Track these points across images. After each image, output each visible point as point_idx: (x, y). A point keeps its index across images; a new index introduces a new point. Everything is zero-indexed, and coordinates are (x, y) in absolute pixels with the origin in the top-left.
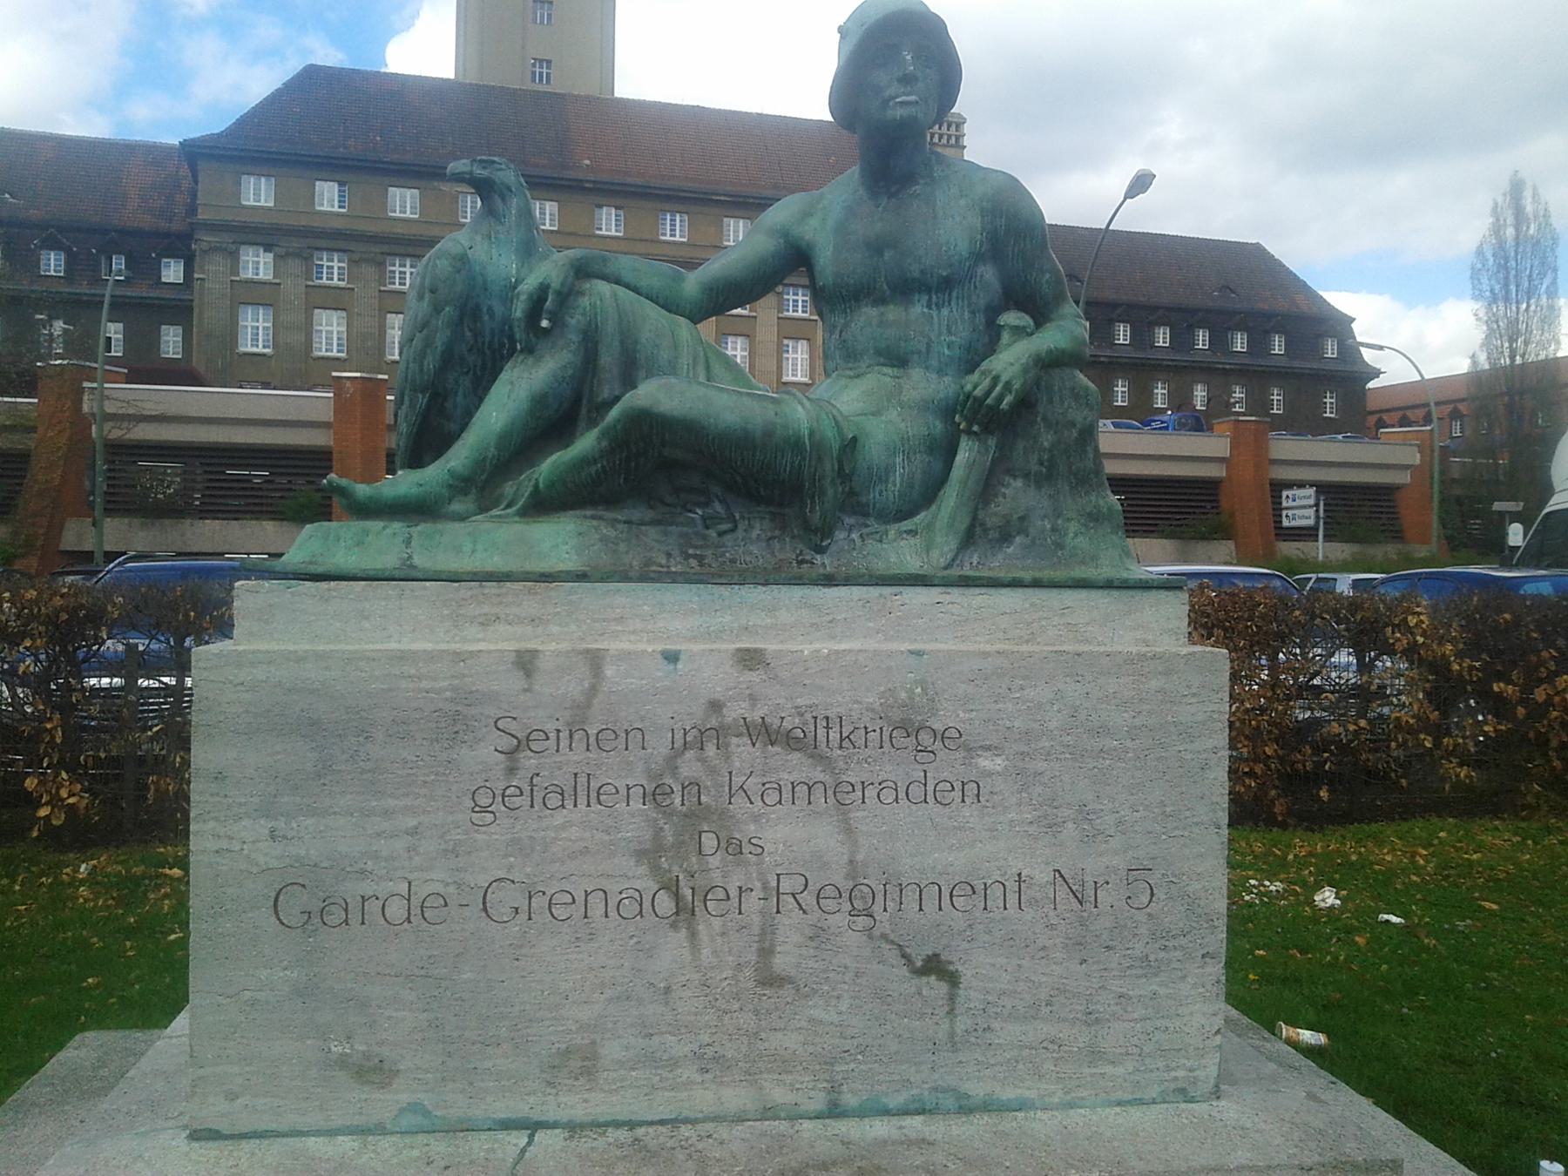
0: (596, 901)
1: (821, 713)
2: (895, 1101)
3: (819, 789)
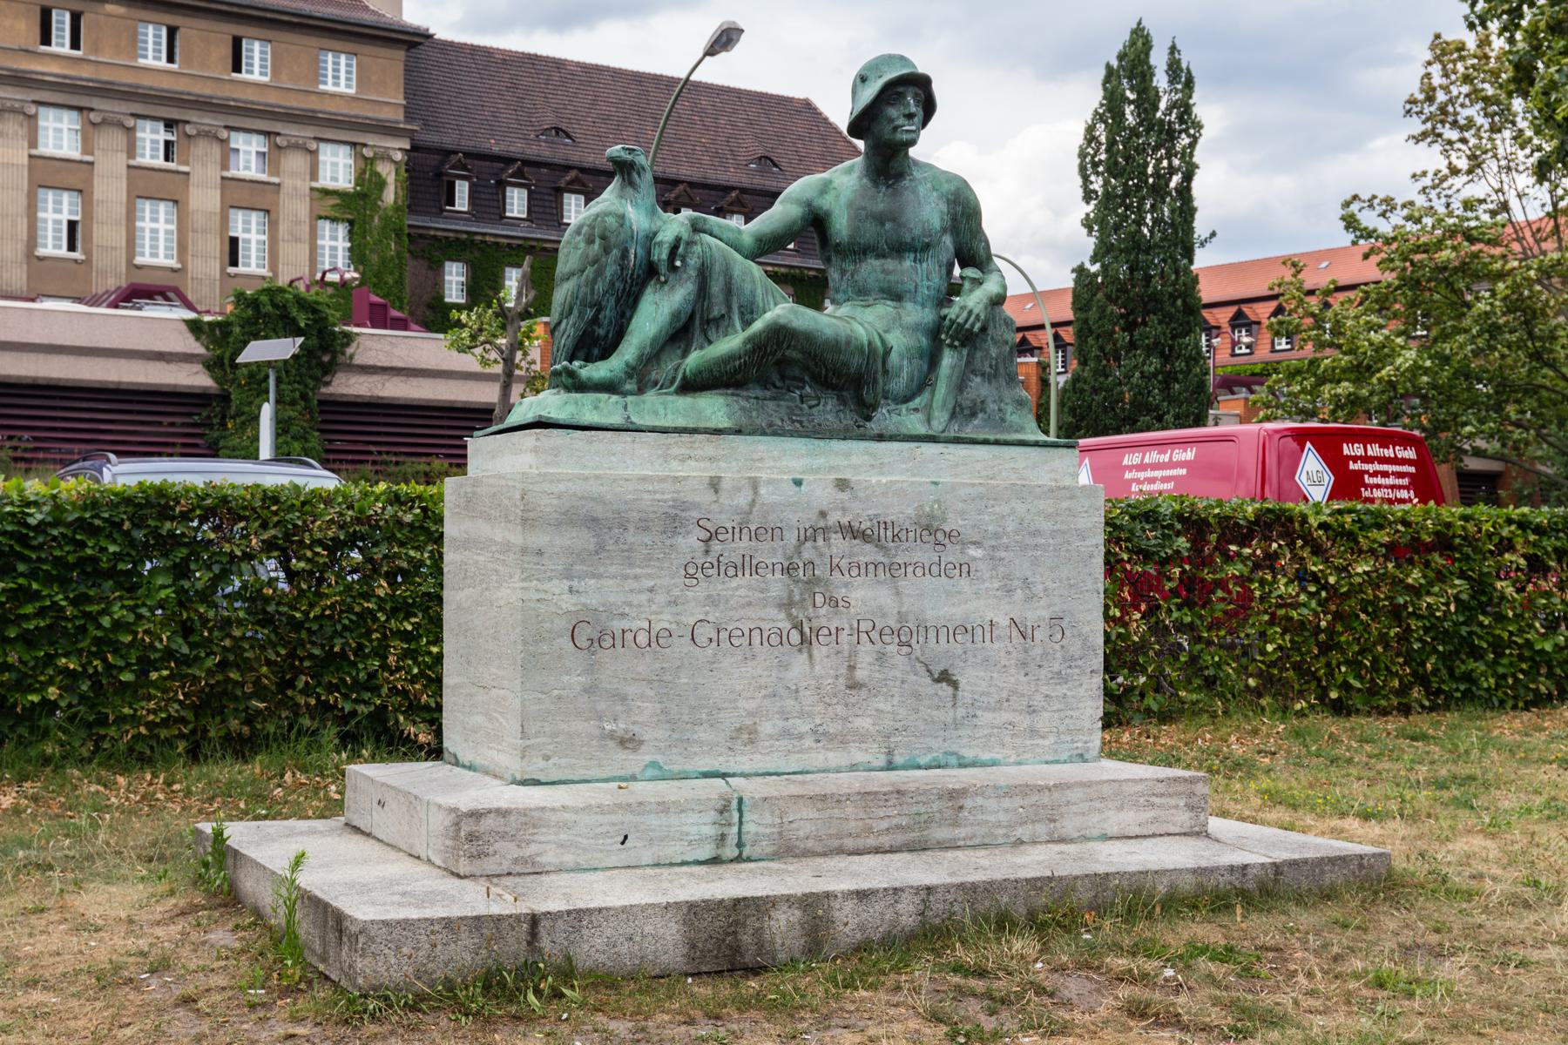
0: (756, 633)
1: (882, 519)
3: (881, 568)
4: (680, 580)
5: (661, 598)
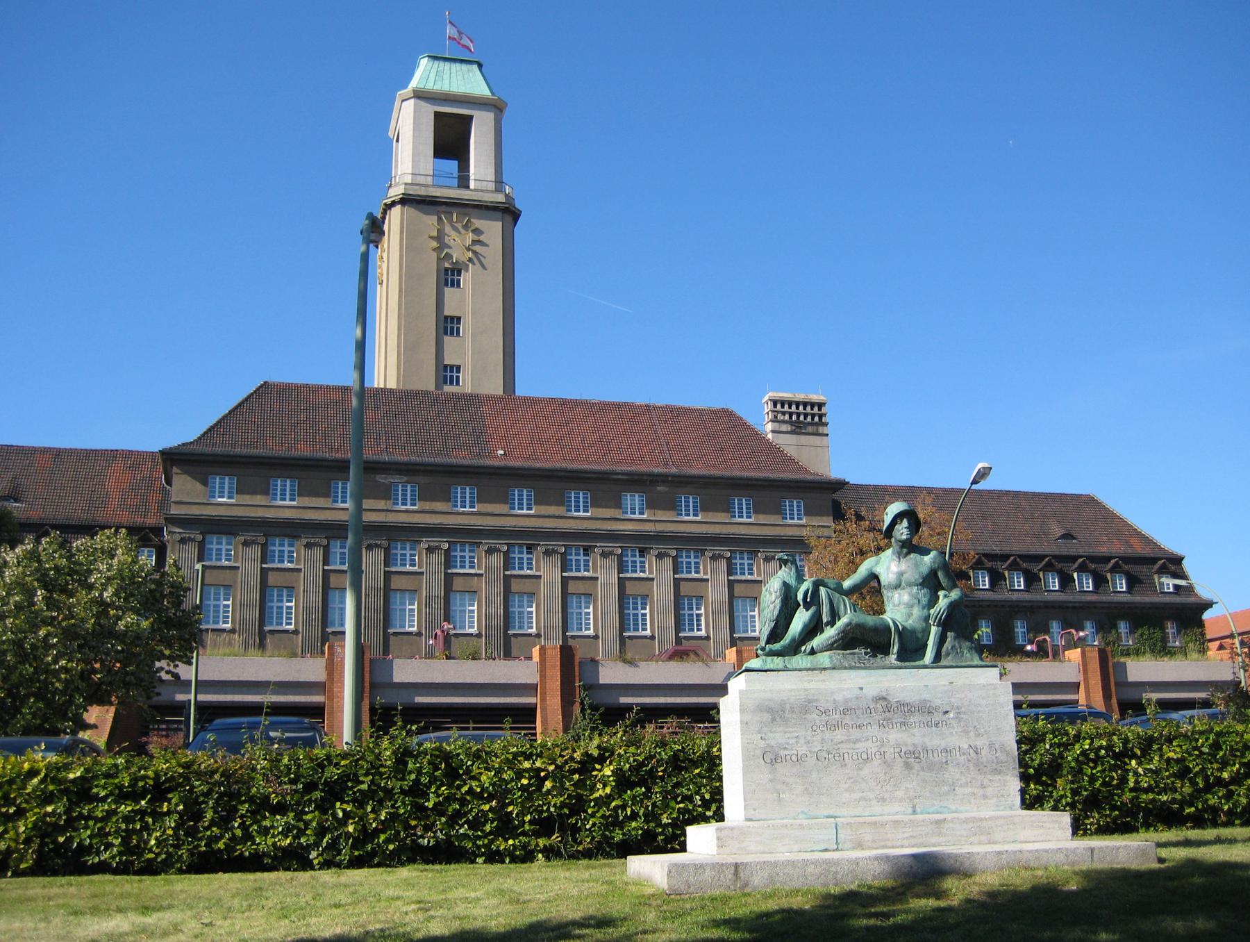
4: (809, 733)
5: (802, 741)
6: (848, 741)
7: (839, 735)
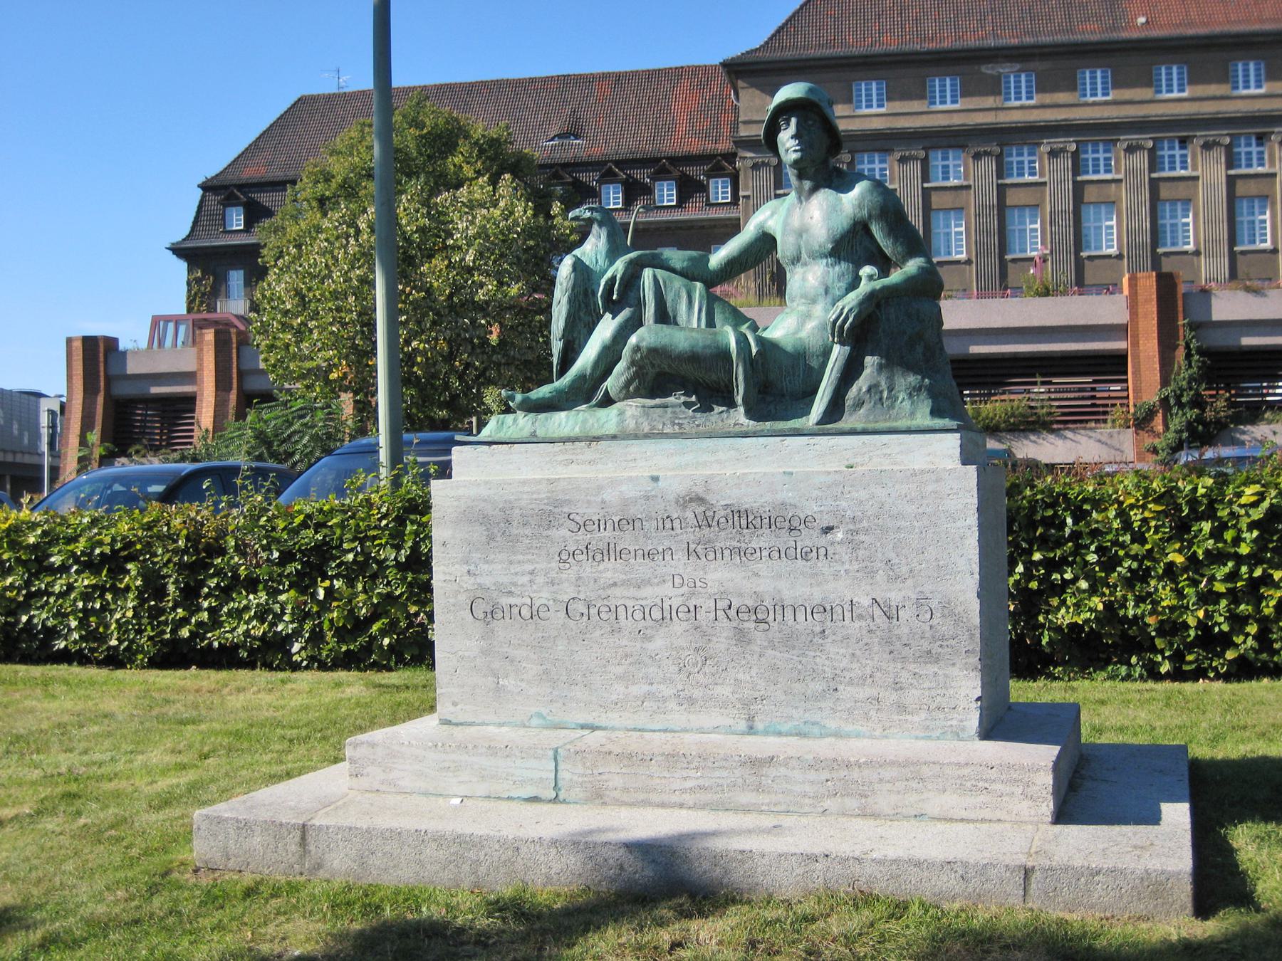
0: (621, 610)
2: (785, 728)
4: (554, 565)
6: (627, 583)
7: (610, 570)
